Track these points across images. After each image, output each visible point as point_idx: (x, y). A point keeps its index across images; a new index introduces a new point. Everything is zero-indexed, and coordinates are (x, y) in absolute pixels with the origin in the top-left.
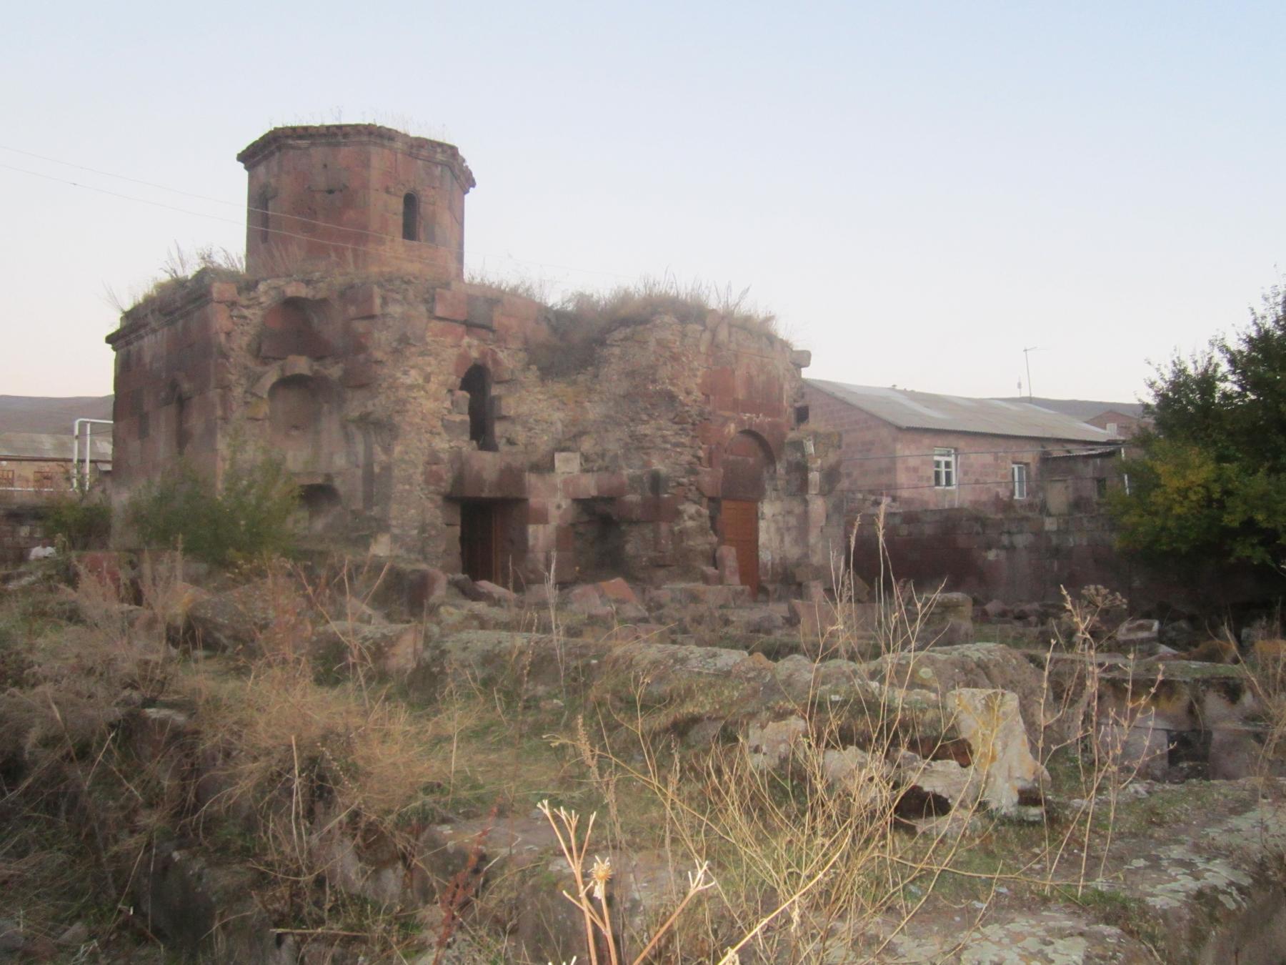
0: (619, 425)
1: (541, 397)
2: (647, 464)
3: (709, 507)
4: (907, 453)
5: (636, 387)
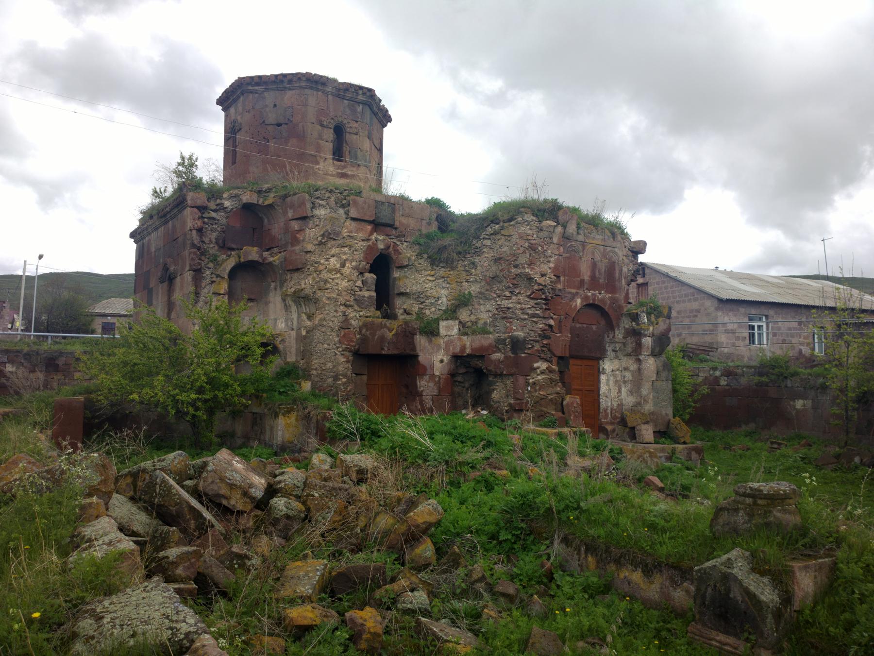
1: (431, 278)
2: (508, 330)
3: (558, 364)
4: (726, 320)
5: (502, 270)
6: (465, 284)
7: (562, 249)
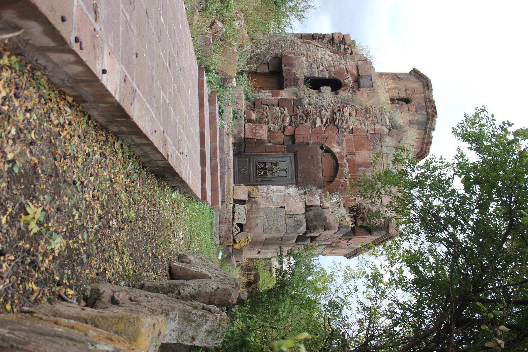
7: (372, 132)
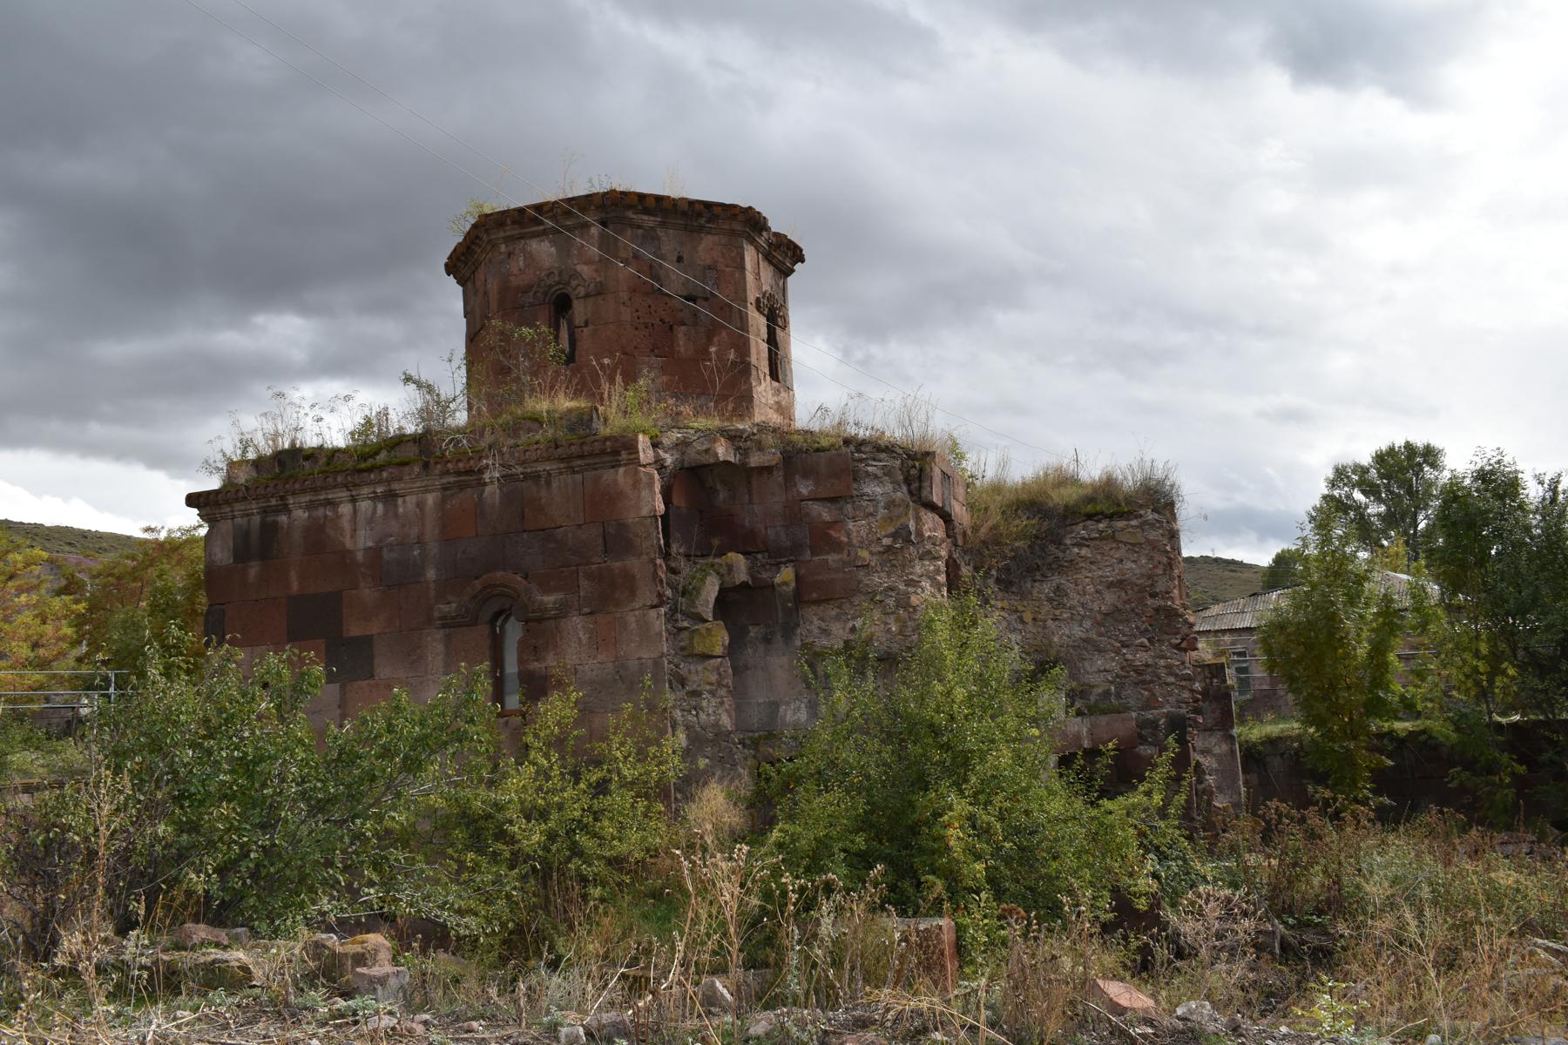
0: (1100, 651)
5: (1128, 601)
6: (1050, 622)
